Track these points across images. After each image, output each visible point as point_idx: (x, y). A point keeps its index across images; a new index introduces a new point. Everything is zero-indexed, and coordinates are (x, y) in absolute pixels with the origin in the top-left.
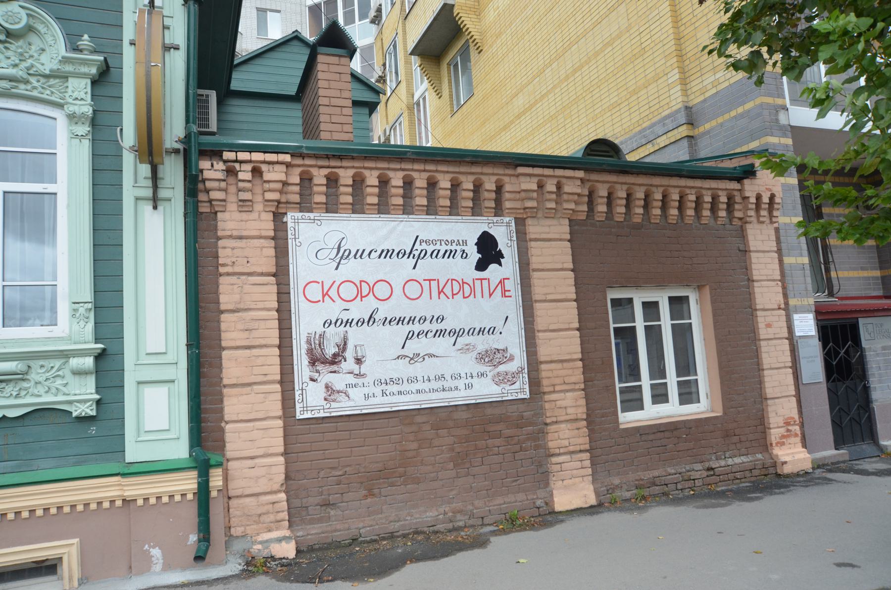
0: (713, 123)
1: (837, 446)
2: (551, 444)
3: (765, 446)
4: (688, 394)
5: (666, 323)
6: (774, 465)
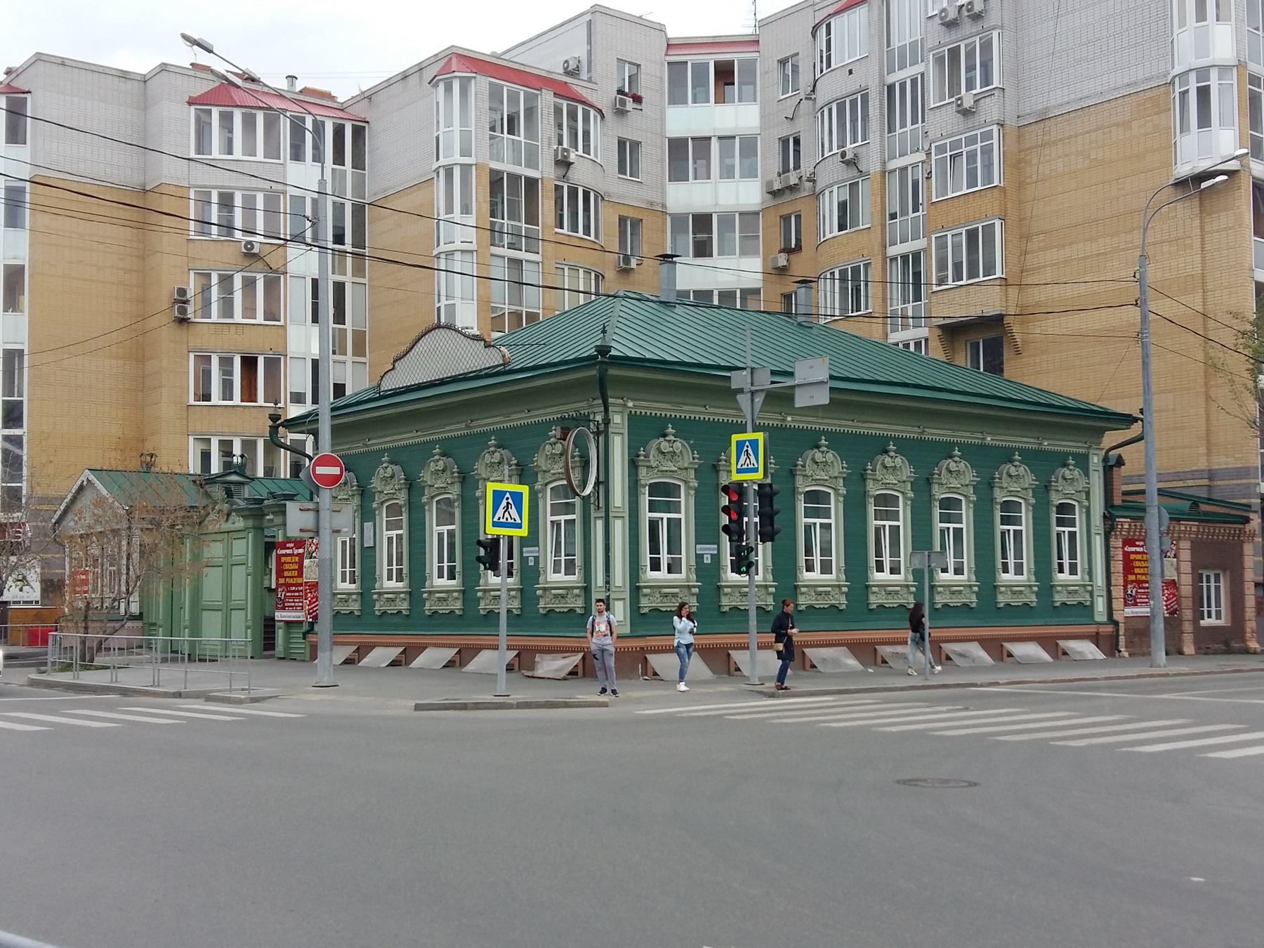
2: (1184, 629)
3: (1243, 640)
4: (1218, 617)
5: (1213, 584)
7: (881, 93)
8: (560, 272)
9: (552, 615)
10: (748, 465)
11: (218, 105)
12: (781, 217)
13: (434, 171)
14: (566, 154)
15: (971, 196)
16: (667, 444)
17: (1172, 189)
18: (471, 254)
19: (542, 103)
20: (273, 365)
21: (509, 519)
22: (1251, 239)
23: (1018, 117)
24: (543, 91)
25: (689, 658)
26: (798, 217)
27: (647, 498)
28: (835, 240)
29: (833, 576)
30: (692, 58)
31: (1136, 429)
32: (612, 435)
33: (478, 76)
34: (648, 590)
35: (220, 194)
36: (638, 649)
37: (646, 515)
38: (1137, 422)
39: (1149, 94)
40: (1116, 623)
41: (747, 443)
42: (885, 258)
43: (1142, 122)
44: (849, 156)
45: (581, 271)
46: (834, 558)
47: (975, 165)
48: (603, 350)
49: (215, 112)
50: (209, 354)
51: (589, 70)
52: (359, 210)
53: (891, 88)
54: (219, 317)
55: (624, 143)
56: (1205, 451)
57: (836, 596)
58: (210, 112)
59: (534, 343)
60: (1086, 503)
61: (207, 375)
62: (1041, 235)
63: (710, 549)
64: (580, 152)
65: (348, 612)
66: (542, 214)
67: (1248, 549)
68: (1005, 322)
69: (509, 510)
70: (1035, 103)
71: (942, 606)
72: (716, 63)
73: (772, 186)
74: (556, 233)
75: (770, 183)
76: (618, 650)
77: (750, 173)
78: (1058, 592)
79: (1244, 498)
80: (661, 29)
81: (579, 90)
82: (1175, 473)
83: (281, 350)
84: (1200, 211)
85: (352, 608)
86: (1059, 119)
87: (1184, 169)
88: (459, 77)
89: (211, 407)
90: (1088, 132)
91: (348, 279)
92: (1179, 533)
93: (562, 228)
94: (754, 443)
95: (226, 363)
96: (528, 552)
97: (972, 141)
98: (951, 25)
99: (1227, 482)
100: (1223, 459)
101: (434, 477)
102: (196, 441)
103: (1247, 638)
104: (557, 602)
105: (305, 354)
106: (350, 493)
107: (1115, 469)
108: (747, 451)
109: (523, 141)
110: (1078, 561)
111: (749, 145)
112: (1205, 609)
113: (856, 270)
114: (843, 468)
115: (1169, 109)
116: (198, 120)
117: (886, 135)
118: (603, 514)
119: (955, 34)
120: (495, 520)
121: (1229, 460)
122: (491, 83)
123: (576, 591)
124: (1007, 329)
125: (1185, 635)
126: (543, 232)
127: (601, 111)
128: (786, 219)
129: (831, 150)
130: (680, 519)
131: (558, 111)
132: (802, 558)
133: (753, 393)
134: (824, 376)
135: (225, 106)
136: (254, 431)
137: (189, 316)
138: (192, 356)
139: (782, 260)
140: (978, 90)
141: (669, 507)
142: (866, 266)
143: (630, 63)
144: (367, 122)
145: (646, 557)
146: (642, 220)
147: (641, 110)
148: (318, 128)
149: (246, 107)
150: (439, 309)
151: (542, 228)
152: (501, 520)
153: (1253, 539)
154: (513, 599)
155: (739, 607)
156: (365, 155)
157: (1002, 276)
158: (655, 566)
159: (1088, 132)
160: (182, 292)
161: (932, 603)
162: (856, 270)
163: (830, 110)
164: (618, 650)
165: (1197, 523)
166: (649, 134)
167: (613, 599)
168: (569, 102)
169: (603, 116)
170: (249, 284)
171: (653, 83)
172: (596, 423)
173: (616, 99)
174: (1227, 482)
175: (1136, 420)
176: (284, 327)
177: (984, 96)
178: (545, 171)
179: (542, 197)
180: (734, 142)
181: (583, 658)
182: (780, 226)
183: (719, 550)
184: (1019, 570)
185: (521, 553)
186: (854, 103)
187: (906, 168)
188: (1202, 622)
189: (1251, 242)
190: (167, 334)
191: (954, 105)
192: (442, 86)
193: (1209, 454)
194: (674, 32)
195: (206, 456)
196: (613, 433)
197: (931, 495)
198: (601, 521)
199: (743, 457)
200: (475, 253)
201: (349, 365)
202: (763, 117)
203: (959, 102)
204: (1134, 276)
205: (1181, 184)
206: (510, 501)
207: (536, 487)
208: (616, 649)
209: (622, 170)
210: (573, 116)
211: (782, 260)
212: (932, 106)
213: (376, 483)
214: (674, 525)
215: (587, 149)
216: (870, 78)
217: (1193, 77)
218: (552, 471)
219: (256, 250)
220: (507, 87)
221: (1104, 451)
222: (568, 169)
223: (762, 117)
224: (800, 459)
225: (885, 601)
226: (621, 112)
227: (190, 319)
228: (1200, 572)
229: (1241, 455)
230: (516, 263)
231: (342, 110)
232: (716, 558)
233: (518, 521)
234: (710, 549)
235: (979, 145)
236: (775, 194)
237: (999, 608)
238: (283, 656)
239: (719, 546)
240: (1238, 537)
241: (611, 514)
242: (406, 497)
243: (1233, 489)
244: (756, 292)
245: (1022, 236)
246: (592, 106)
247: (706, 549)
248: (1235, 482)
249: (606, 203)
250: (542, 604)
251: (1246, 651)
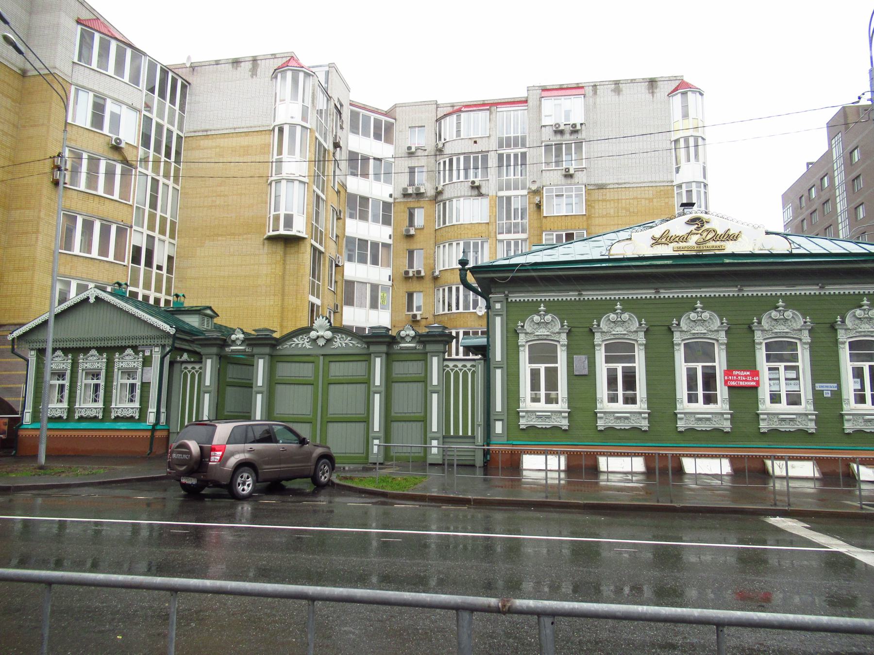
20: (121, 232)
34: (683, 416)
39: (662, 188)
44: (477, 184)
50: (76, 215)
52: (179, 138)
89: (74, 257)
96: (823, 387)
119: (559, 137)
136: (105, 280)
163: (458, 160)
186: (476, 159)
192: (289, 74)
200: (306, 185)
236: (406, 195)
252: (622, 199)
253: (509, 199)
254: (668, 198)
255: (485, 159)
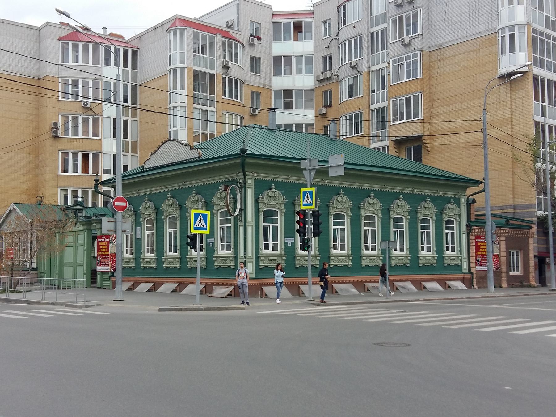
0: (520, 211)
1: (540, 284)
3: (529, 281)
4: (518, 271)
5: (515, 256)
6: (531, 285)
7: (368, 36)
8: (224, 116)
9: (220, 269)
10: (308, 202)
11: (72, 41)
12: (323, 91)
13: (168, 70)
14: (227, 63)
15: (408, 82)
16: (272, 193)
17: (497, 80)
18: (184, 108)
19: (216, 40)
20: (96, 157)
21: (201, 226)
22: (533, 102)
23: (429, 47)
24: (217, 35)
25: (281, 288)
26: (331, 92)
27: (263, 217)
28: (347, 102)
29: (346, 252)
30: (283, 21)
31: (481, 187)
32: (247, 189)
33: (188, 28)
34: (263, 258)
35: (73, 81)
36: (259, 284)
37: (262, 225)
38: (481, 184)
39: (487, 37)
40: (472, 274)
41: (308, 193)
42: (369, 110)
43: (484, 49)
44: (353, 64)
45: (234, 115)
46: (346, 244)
47: (410, 69)
48: (243, 151)
49: (71, 44)
50: (68, 152)
51: (238, 26)
52: (134, 88)
53: (372, 34)
54: (72, 135)
55: (253, 58)
56: (512, 197)
57: (347, 261)
58: (68, 44)
59: (212, 147)
60: (459, 220)
61: (66, 161)
62: (439, 100)
63: (291, 240)
64: (234, 62)
65: (129, 267)
66: (216, 90)
67: (531, 240)
68: (423, 139)
69: (201, 222)
70: (436, 41)
71: (394, 265)
72: (294, 23)
73: (319, 78)
74: (222, 98)
75: (318, 77)
76: (250, 285)
77: (309, 72)
78: (446, 259)
79: (529, 218)
80: (270, 7)
81: (233, 34)
82: (498, 206)
83: (100, 150)
84: (510, 89)
85: (131, 266)
86: (447, 48)
87: (503, 71)
88: (179, 28)
89: (68, 176)
90: (460, 54)
91: (129, 118)
92: (500, 233)
93: (225, 96)
94: (311, 193)
95: (75, 156)
96: (209, 241)
97: (408, 58)
98: (399, 6)
99: (522, 211)
100: (520, 200)
101: (168, 207)
102: (61, 191)
103: (531, 280)
104: (223, 263)
105: (110, 152)
106: (130, 214)
107: (472, 204)
108: (307, 196)
109: (208, 57)
110: (455, 246)
111: (309, 59)
112: (512, 267)
113: (356, 115)
114: (350, 203)
115: (497, 44)
116: (63, 47)
117: (370, 55)
118: (243, 224)
119: (401, 10)
120: (195, 226)
121: (523, 200)
122: (194, 31)
123: (231, 258)
124: (424, 142)
125: (503, 279)
126: (217, 98)
127: (243, 44)
128: (325, 92)
129: (345, 61)
130: (278, 226)
131: (224, 44)
132: (332, 244)
133: (310, 170)
134: (342, 163)
135: (75, 41)
136: (87, 186)
137: (58, 135)
138: (60, 152)
139: (323, 111)
140: (411, 35)
141: (272, 221)
142: (361, 113)
143: (256, 23)
144: (139, 49)
145: (262, 243)
146: (261, 93)
147: (261, 43)
148: (117, 51)
149: (84, 41)
150: (170, 132)
151: (216, 96)
152: (198, 226)
153: (533, 236)
154: (203, 262)
155: (304, 266)
156: (137, 63)
157: (422, 118)
158: (266, 247)
159: (460, 54)
160: (56, 124)
161: (390, 264)
162: (356, 115)
163: (345, 44)
164: (250, 285)
165: (508, 229)
166: (264, 55)
167: (248, 262)
168: (229, 40)
169: (244, 46)
170: (85, 121)
171: (266, 31)
172: (240, 183)
173: (249, 39)
174: (522, 211)
175: (481, 183)
176: (101, 140)
177: (414, 38)
178: (218, 71)
179: (216, 82)
180: (302, 58)
181: (234, 288)
182: (323, 96)
183: (295, 240)
184: (429, 249)
185: (207, 241)
186: (356, 41)
187: (379, 70)
188: (511, 273)
189: (533, 103)
190: (49, 143)
191: (401, 42)
192: (172, 33)
193: (514, 198)
194: (275, 9)
195: (66, 198)
196: (248, 188)
197: (389, 216)
198: (242, 227)
199: (306, 199)
200: (186, 107)
201: (130, 157)
202: (315, 47)
203: (403, 40)
204: (481, 119)
205: (502, 77)
206: (202, 218)
207: (213, 212)
208: (249, 284)
209: (252, 70)
210: (230, 46)
211: (323, 111)
212: (391, 42)
213: (142, 210)
214: (275, 229)
215: (236, 61)
216: (363, 30)
217: (507, 30)
218: (220, 205)
219: (88, 106)
220: (201, 33)
221: (467, 196)
222: (228, 70)
223: (315, 47)
224: (331, 200)
225: (369, 263)
226: (252, 45)
227: (59, 136)
228: (510, 251)
229: (528, 199)
230: (205, 112)
231: (127, 43)
232: (294, 244)
233: (205, 227)
234: (291, 240)
235: (412, 59)
236: (320, 81)
237: (420, 266)
238: (100, 287)
239: (295, 238)
240: (527, 235)
241: (247, 224)
242: (155, 216)
243: (524, 213)
244: (312, 125)
245: (431, 101)
246: (239, 42)
247: (289, 240)
248: (525, 210)
249: (245, 85)
250: (216, 264)
251: (530, 286)
252: (455, 56)
253: (378, 71)
254: (491, 46)
255: (361, 39)
